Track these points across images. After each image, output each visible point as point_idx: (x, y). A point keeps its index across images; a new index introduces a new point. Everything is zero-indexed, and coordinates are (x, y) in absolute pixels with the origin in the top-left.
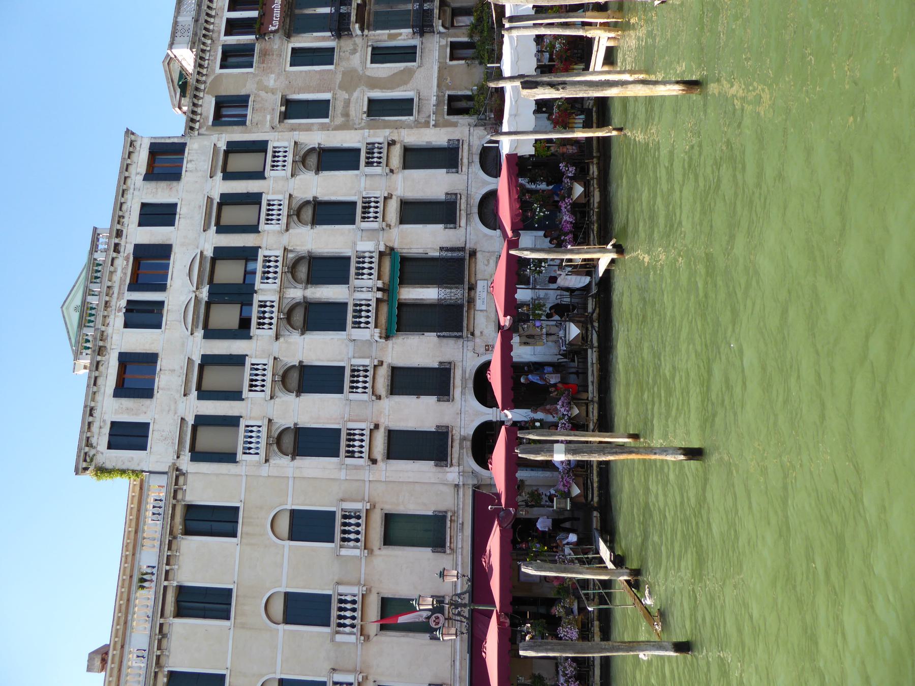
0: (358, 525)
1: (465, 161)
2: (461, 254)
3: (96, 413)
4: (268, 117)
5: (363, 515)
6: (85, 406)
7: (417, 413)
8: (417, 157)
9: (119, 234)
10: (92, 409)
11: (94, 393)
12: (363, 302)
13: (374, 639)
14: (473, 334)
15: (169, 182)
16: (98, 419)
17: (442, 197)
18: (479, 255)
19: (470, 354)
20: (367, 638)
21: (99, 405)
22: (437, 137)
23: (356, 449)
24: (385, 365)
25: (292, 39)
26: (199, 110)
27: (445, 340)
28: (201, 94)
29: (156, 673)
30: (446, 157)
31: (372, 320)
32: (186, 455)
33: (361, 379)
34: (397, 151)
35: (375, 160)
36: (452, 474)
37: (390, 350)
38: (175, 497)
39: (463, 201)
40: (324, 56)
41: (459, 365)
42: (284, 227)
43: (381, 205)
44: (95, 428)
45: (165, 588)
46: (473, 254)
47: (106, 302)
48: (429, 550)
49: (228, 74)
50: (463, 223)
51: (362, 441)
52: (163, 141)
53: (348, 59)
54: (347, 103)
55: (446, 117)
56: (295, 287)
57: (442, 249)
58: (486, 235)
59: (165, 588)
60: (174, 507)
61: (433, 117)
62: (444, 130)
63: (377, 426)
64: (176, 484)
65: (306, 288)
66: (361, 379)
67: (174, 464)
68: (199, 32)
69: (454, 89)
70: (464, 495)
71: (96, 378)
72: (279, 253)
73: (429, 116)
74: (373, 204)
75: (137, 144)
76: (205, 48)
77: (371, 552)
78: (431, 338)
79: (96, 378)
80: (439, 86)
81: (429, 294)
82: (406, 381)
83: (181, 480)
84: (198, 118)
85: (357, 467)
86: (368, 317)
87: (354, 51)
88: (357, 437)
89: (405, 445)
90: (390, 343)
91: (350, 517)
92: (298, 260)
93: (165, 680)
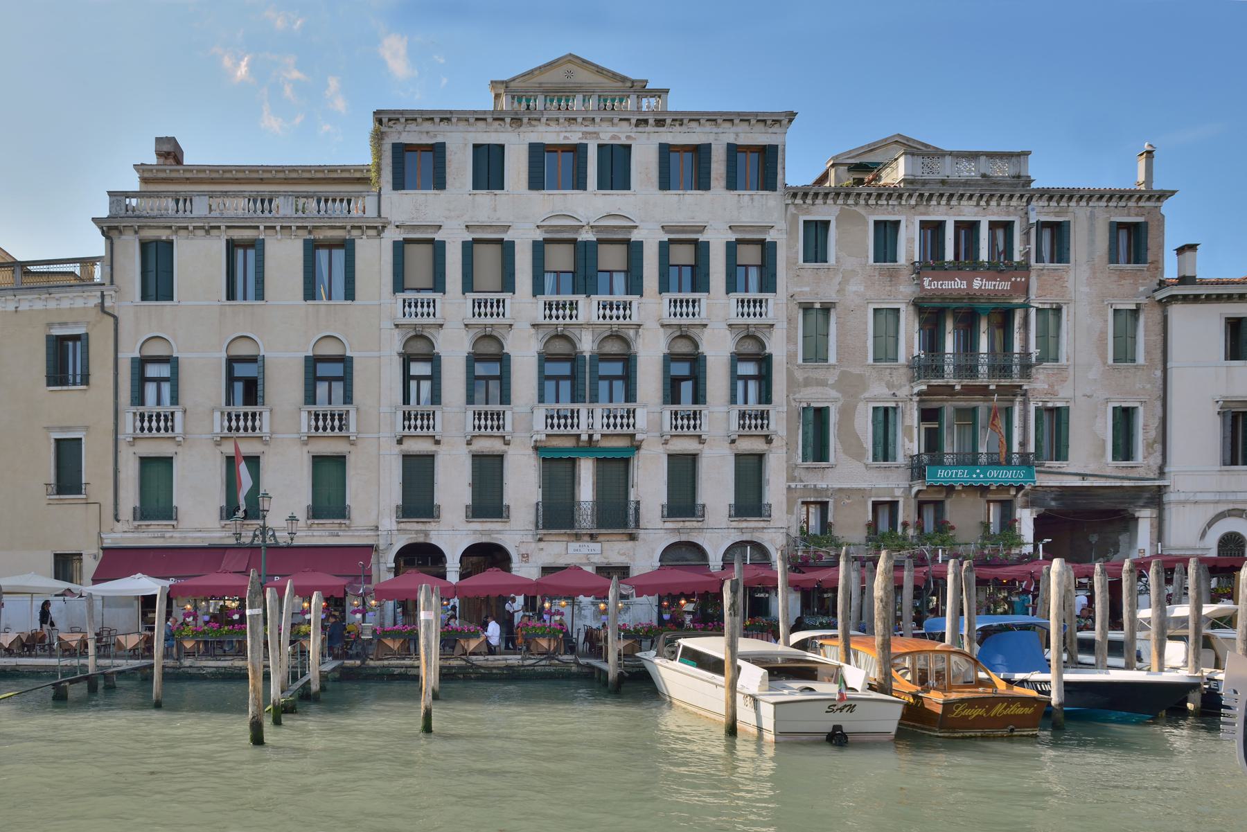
1: (744, 525)
2: (632, 524)
3: (444, 125)
6: (451, 112)
7: (453, 485)
9: (660, 123)
10: (448, 120)
12: (576, 420)
15: (724, 176)
16: (438, 128)
17: (700, 500)
18: (630, 544)
19: (518, 538)
20: (218, 444)
22: (775, 491)
23: (413, 422)
24: (505, 448)
26: (819, 201)
27: (533, 511)
28: (840, 201)
30: (749, 502)
32: (399, 236)
33: (489, 422)
35: (747, 422)
36: (389, 523)
38: (353, 227)
39: (695, 524)
41: (507, 527)
44: (428, 126)
45: (258, 227)
46: (632, 537)
47: (575, 119)
49: (866, 232)
50: (669, 525)
54: (822, 383)
55: (800, 501)
57: (638, 503)
58: (653, 550)
59: (258, 227)
60: (343, 228)
61: (800, 485)
63: (438, 442)
64: (368, 227)
66: (489, 422)
68: (927, 187)
69: (835, 508)
75: (776, 128)
77: (305, 443)
78: (536, 495)
80: (840, 490)
81: (586, 492)
84: (809, 201)
86: (559, 426)
88: (425, 422)
90: (531, 451)
92: (625, 341)
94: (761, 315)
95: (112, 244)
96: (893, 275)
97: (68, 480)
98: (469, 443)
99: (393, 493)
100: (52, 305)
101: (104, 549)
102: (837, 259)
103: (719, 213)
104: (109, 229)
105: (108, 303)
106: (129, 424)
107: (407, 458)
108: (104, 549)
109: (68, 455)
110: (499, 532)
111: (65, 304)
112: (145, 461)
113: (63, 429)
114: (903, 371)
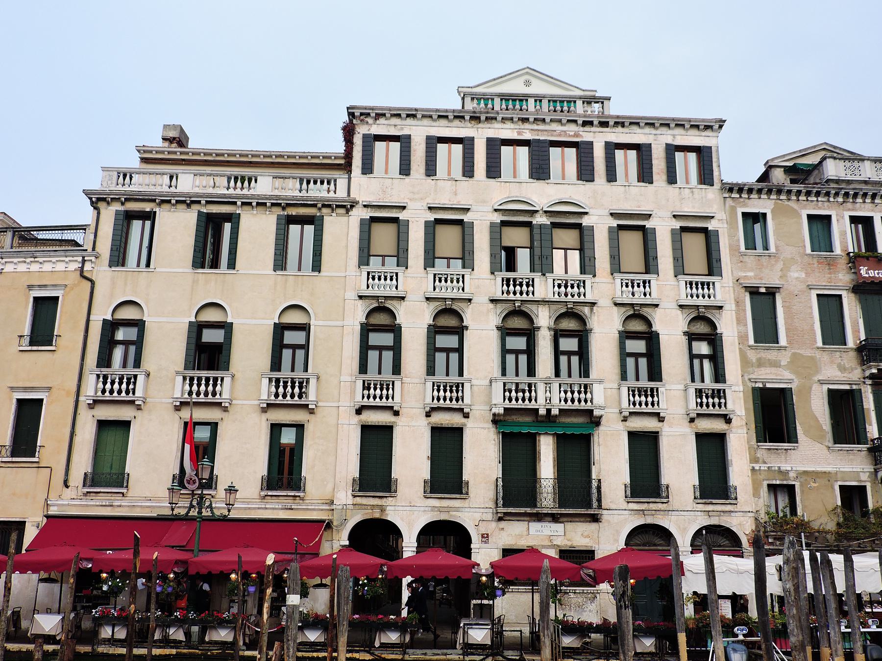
0: (292, 396)
1: (710, 508)
2: (595, 504)
3: (410, 121)
4: (751, 274)
5: (303, 402)
6: (416, 110)
7: (411, 458)
8: (712, 450)
9: (604, 124)
10: (414, 116)
11: (431, 117)
12: (533, 394)
13: (176, 416)
14: (500, 519)
15: (665, 171)
16: (404, 122)
17: (664, 481)
18: (594, 526)
19: (478, 516)
20: (177, 409)
21: (419, 123)
23: (372, 391)
24: (464, 420)
25: (852, 296)
26: (754, 196)
27: (493, 487)
28: (773, 197)
29: (154, 201)
30: (714, 483)
31: (514, 404)
32: (367, 214)
33: (448, 394)
34: (717, 426)
35: (705, 400)
36: (344, 497)
37: (482, 425)
38: (324, 206)
39: (660, 506)
40: (833, 332)
41: (465, 503)
42: (619, 301)
43: (650, 409)
44: (395, 121)
45: (235, 203)
46: (595, 519)
47: (527, 119)
48: (265, 472)
49: (801, 224)
51: (381, 398)
52: (714, 160)
53: (832, 362)
54: (775, 364)
55: (765, 483)
56: (550, 317)
57: (599, 481)
58: (618, 532)
59: (235, 203)
60: (315, 206)
61: (764, 467)
62: (749, 481)
63: (397, 413)
64: (337, 206)
65: (549, 329)
66: (448, 394)
67: (357, 203)
68: (852, 186)
69: (802, 492)
70: (322, 510)
71: (447, 117)
72: (589, 298)
73: (765, 463)
74: (650, 399)
75: (708, 133)
76: (832, 196)
77: (264, 410)
78: (496, 471)
79: (447, 117)
80: (805, 472)
81: (547, 469)
82: (447, 444)
83: (342, 211)
84: (745, 195)
85: (353, 392)
86: (517, 400)
87: (842, 369)
88: (385, 392)
89: (376, 443)
90: (490, 425)
91: (301, 387)
92: (581, 319)
93: (148, 210)
94: (709, 297)
95: (99, 213)
96: (831, 263)
97: (24, 441)
98: (428, 415)
99: (350, 464)
100: (35, 267)
101: (47, 517)
102: (777, 247)
103: (664, 204)
104: (97, 200)
105: (88, 267)
106: (91, 387)
107: (366, 429)
108: (47, 517)
109: (28, 413)
110: (457, 509)
111: (47, 267)
112: (103, 425)
113: (26, 389)
114: (853, 354)
